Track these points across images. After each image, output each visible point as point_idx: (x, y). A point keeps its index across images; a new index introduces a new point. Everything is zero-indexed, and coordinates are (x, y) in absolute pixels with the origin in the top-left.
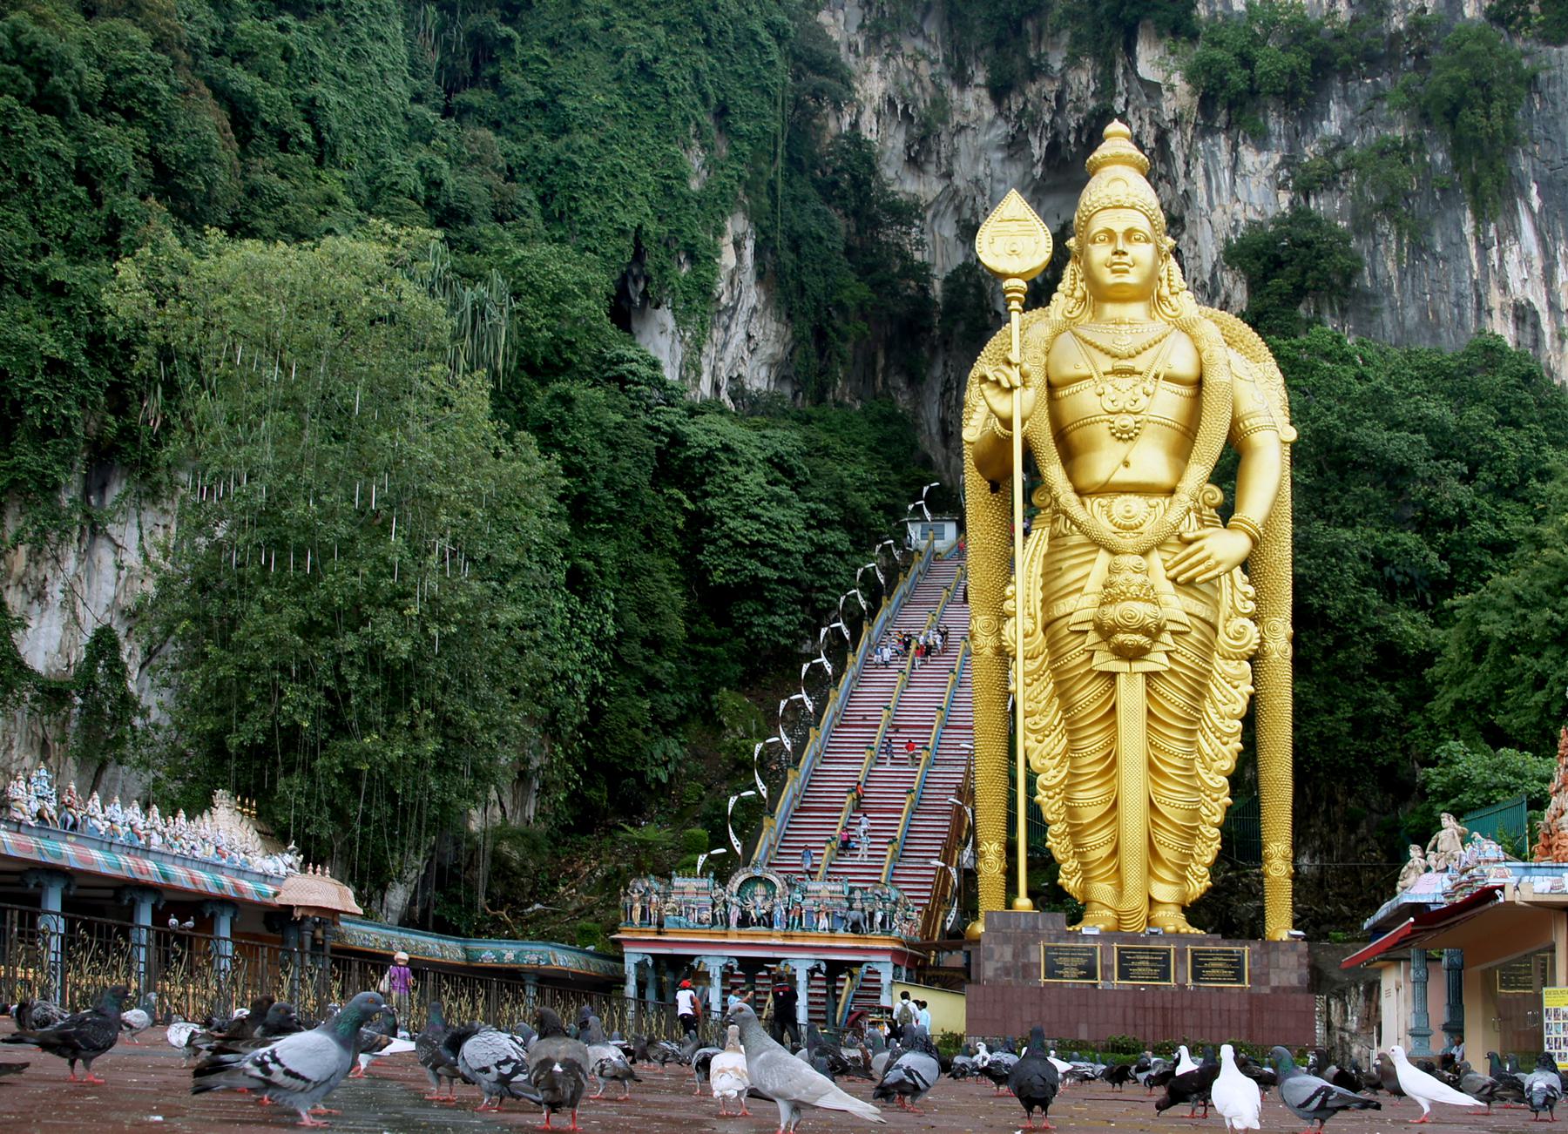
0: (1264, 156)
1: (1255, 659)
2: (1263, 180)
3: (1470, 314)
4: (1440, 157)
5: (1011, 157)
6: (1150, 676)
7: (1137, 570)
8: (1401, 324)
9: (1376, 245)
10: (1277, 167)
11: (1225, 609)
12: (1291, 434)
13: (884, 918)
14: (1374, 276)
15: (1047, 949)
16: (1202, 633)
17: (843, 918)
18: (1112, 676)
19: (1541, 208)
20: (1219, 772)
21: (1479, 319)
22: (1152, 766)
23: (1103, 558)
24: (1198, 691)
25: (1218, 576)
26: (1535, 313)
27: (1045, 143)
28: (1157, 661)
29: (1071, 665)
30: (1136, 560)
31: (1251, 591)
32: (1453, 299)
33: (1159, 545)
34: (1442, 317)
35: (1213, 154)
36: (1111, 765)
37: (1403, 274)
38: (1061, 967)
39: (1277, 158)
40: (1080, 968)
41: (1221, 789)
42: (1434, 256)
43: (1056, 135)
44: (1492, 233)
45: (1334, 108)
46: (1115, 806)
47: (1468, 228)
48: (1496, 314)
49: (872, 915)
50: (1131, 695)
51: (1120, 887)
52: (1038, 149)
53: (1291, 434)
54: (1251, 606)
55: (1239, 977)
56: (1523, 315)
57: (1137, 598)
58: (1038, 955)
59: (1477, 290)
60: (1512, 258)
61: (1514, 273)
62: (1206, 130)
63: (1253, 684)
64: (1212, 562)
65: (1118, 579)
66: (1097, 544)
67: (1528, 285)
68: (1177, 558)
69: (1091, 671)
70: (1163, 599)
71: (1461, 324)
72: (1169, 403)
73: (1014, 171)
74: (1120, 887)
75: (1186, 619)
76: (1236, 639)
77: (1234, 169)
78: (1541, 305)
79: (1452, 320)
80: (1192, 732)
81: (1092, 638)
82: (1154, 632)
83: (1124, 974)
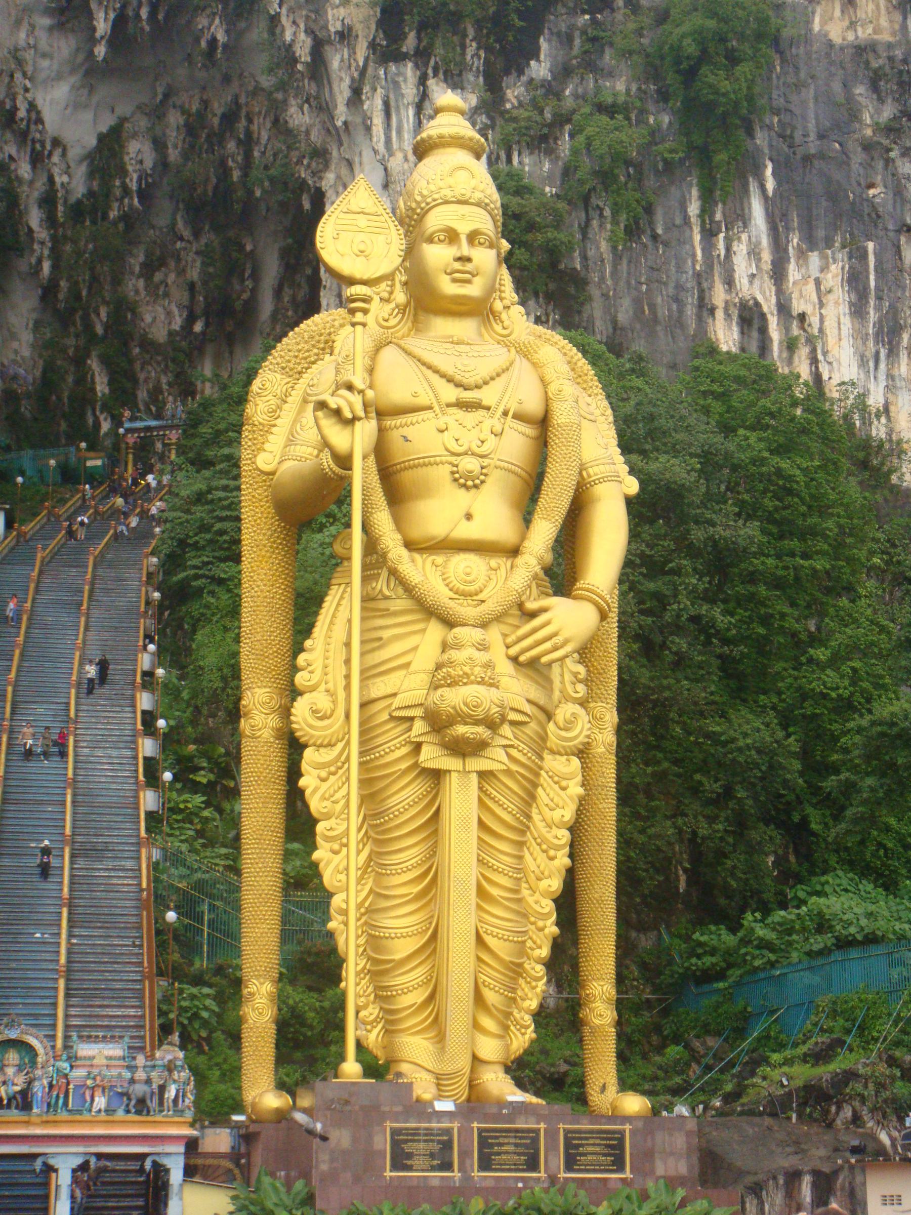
1: (583, 753)
3: (690, 311)
4: (666, 119)
5: (60, 26)
6: (484, 775)
7: (483, 647)
8: (614, 322)
9: (588, 221)
11: (557, 694)
12: (633, 486)
13: (178, 1091)
14: (585, 258)
15: (395, 1132)
16: (540, 723)
17: (122, 1094)
18: (436, 776)
19: (775, 191)
21: (700, 319)
26: (763, 316)
27: (112, 16)
28: (495, 759)
29: (388, 759)
30: (476, 634)
31: (581, 669)
32: (671, 290)
33: (498, 618)
34: (660, 314)
35: (396, 84)
36: (431, 883)
37: (617, 257)
38: (410, 1156)
40: (432, 1156)
41: (548, 915)
42: (655, 237)
43: (124, 7)
44: (718, 216)
45: (544, 45)
46: (434, 936)
47: (694, 209)
48: (720, 314)
49: (162, 1089)
50: (461, 799)
51: (441, 1038)
52: (102, 26)
53: (633, 486)
54: (581, 689)
55: (619, 1165)
56: (750, 317)
57: (482, 682)
58: (383, 1142)
59: (699, 284)
60: (741, 249)
61: (742, 266)
62: (387, 52)
63: (583, 785)
65: (453, 654)
66: (430, 611)
67: (757, 282)
68: (521, 632)
69: (416, 765)
70: (504, 681)
71: (679, 322)
72: (515, 444)
73: (63, 43)
74: (441, 1038)
75: (527, 708)
76: (566, 729)
77: (419, 108)
78: (769, 305)
79: (670, 317)
80: (521, 844)
81: (419, 727)
82: (492, 725)
83: (485, 1164)
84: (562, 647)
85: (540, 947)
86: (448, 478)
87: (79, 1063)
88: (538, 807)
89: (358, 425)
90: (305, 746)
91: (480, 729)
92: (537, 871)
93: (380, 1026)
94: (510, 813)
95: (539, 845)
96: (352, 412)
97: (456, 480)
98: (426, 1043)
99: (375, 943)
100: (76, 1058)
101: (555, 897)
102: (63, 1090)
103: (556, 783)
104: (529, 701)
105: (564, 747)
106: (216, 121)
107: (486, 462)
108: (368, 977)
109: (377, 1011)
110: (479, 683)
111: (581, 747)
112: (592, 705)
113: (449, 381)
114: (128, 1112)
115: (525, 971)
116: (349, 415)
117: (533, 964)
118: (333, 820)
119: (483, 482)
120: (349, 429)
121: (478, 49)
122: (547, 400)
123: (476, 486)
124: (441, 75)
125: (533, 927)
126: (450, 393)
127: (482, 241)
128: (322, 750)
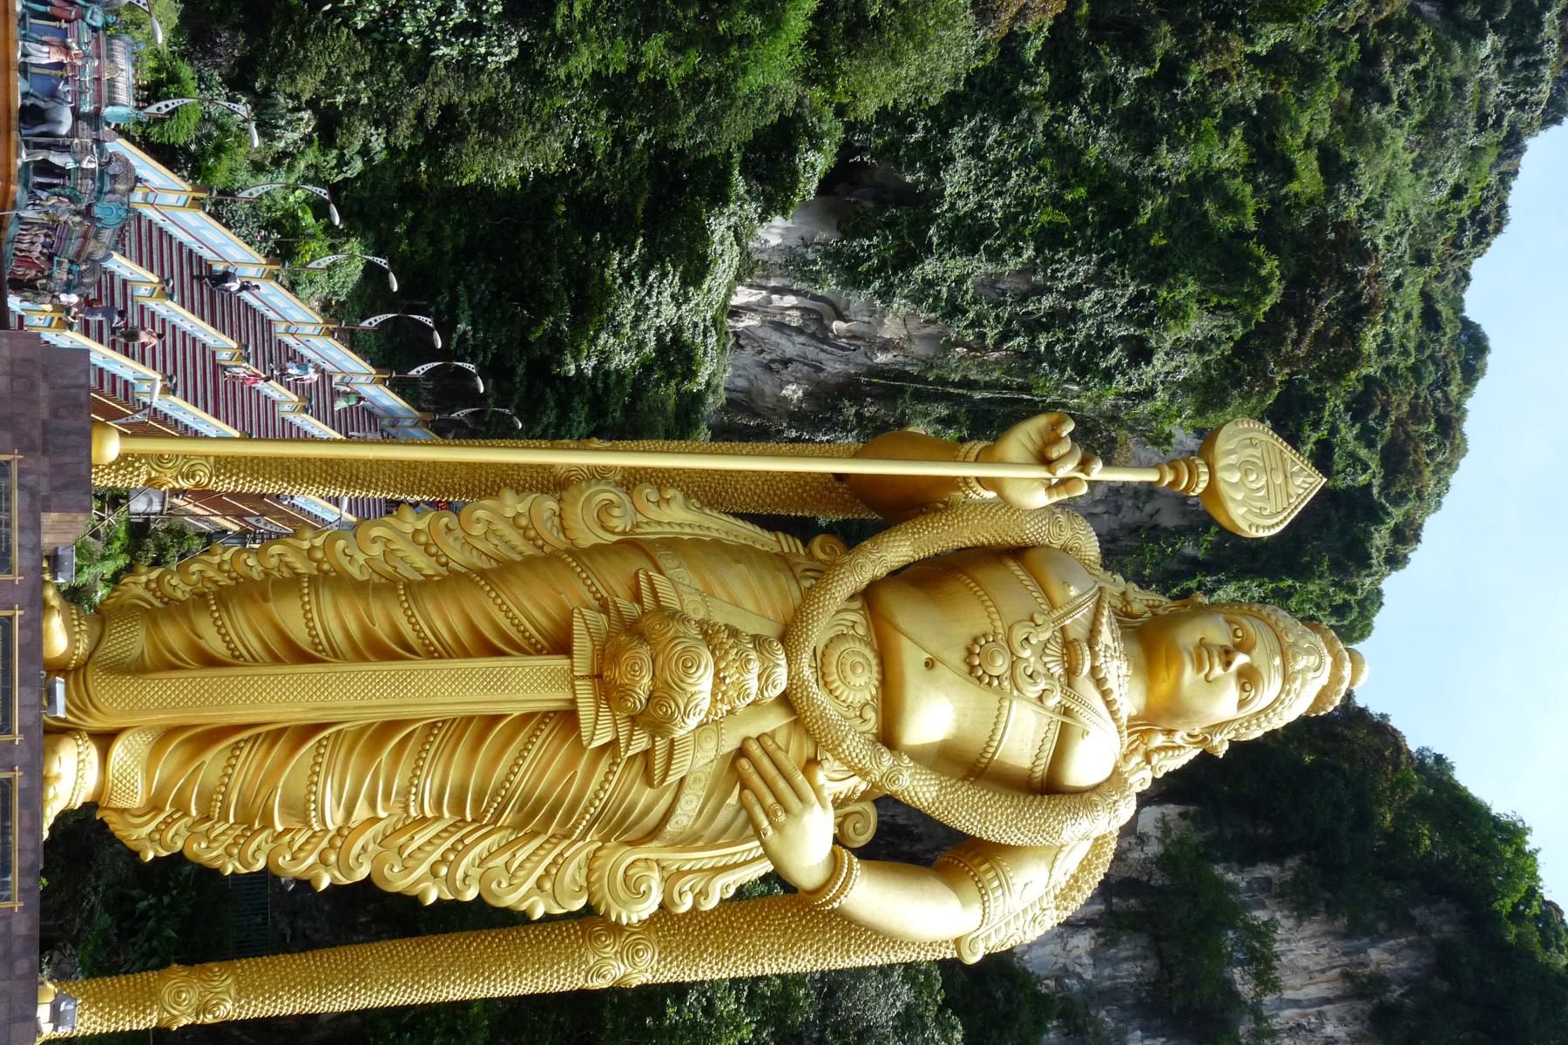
0: (1086, 960)
2: (1061, 960)
10: (1079, 977)
20: (377, 861)
22: (390, 727)
23: (768, 629)
24: (536, 816)
25: (758, 833)
28: (599, 729)
31: (710, 904)
39: (1088, 976)
49: (65, 149)
50: (529, 685)
54: (685, 905)
57: (719, 679)
63: (548, 918)
64: (781, 817)
68: (781, 756)
75: (673, 779)
81: (630, 608)
84: (771, 823)
85: (293, 859)
86: (977, 631)
87: (103, 40)
88: (508, 843)
89: (1041, 473)
90: (560, 500)
91: (647, 680)
92: (414, 846)
93: (157, 603)
94: (511, 772)
95: (453, 848)
96: (1060, 458)
97: (975, 641)
98: (136, 652)
99: (290, 584)
100: (111, 37)
101: (375, 879)
102: (58, 12)
103: (547, 870)
104: (682, 780)
105: (600, 879)
106: (905, 848)
107: (1006, 684)
108: (233, 583)
109: (179, 594)
110: (716, 674)
111: (602, 909)
112: (653, 937)
113: (1091, 631)
114: (25, 95)
115: (256, 833)
116: (1055, 453)
117: (266, 848)
118: (459, 533)
119: (979, 678)
120: (1032, 460)
121: (1137, 975)
122: (1079, 792)
123: (972, 669)
124: (1102, 940)
125: (324, 844)
126: (1078, 631)
127: (1248, 687)
128: (556, 520)
